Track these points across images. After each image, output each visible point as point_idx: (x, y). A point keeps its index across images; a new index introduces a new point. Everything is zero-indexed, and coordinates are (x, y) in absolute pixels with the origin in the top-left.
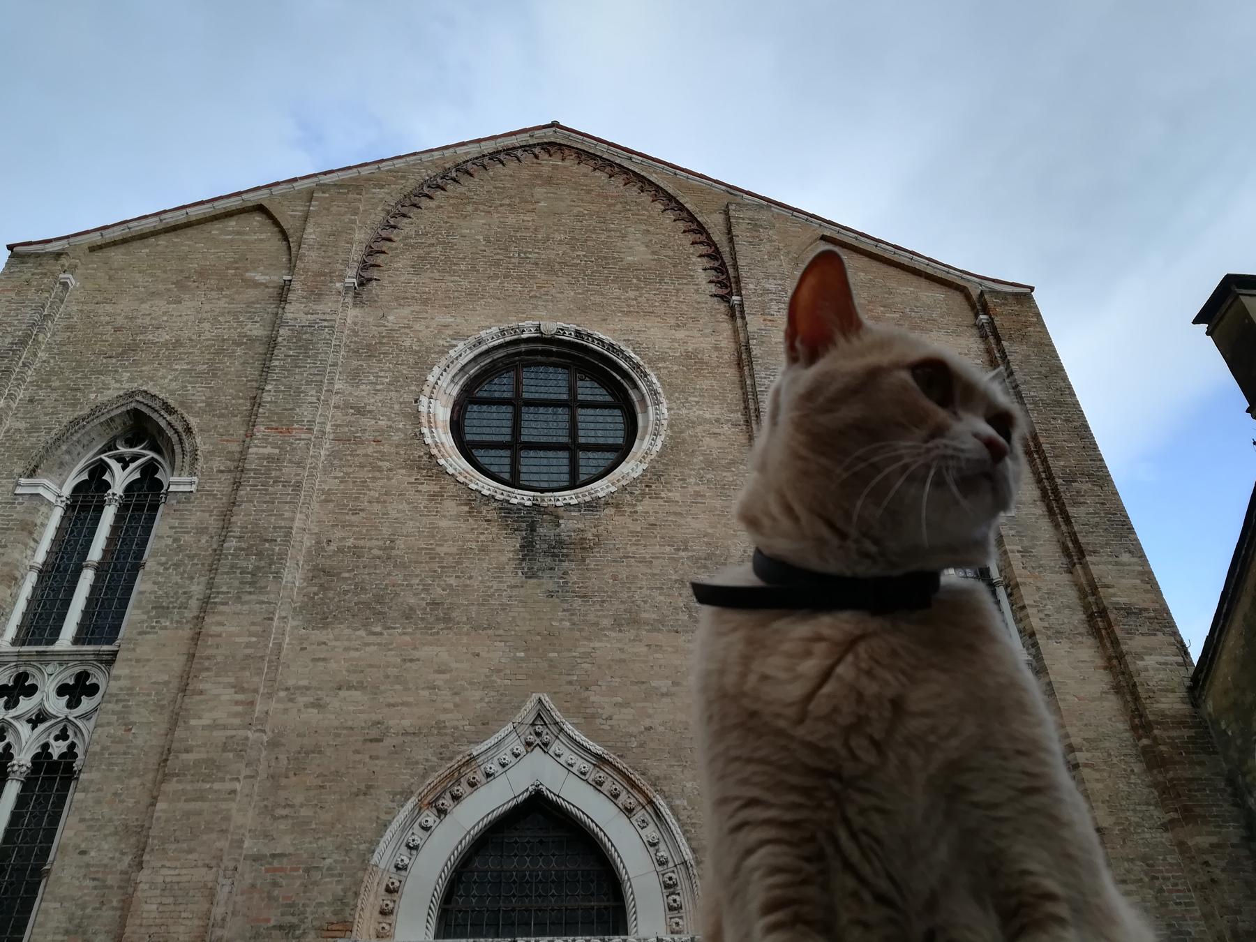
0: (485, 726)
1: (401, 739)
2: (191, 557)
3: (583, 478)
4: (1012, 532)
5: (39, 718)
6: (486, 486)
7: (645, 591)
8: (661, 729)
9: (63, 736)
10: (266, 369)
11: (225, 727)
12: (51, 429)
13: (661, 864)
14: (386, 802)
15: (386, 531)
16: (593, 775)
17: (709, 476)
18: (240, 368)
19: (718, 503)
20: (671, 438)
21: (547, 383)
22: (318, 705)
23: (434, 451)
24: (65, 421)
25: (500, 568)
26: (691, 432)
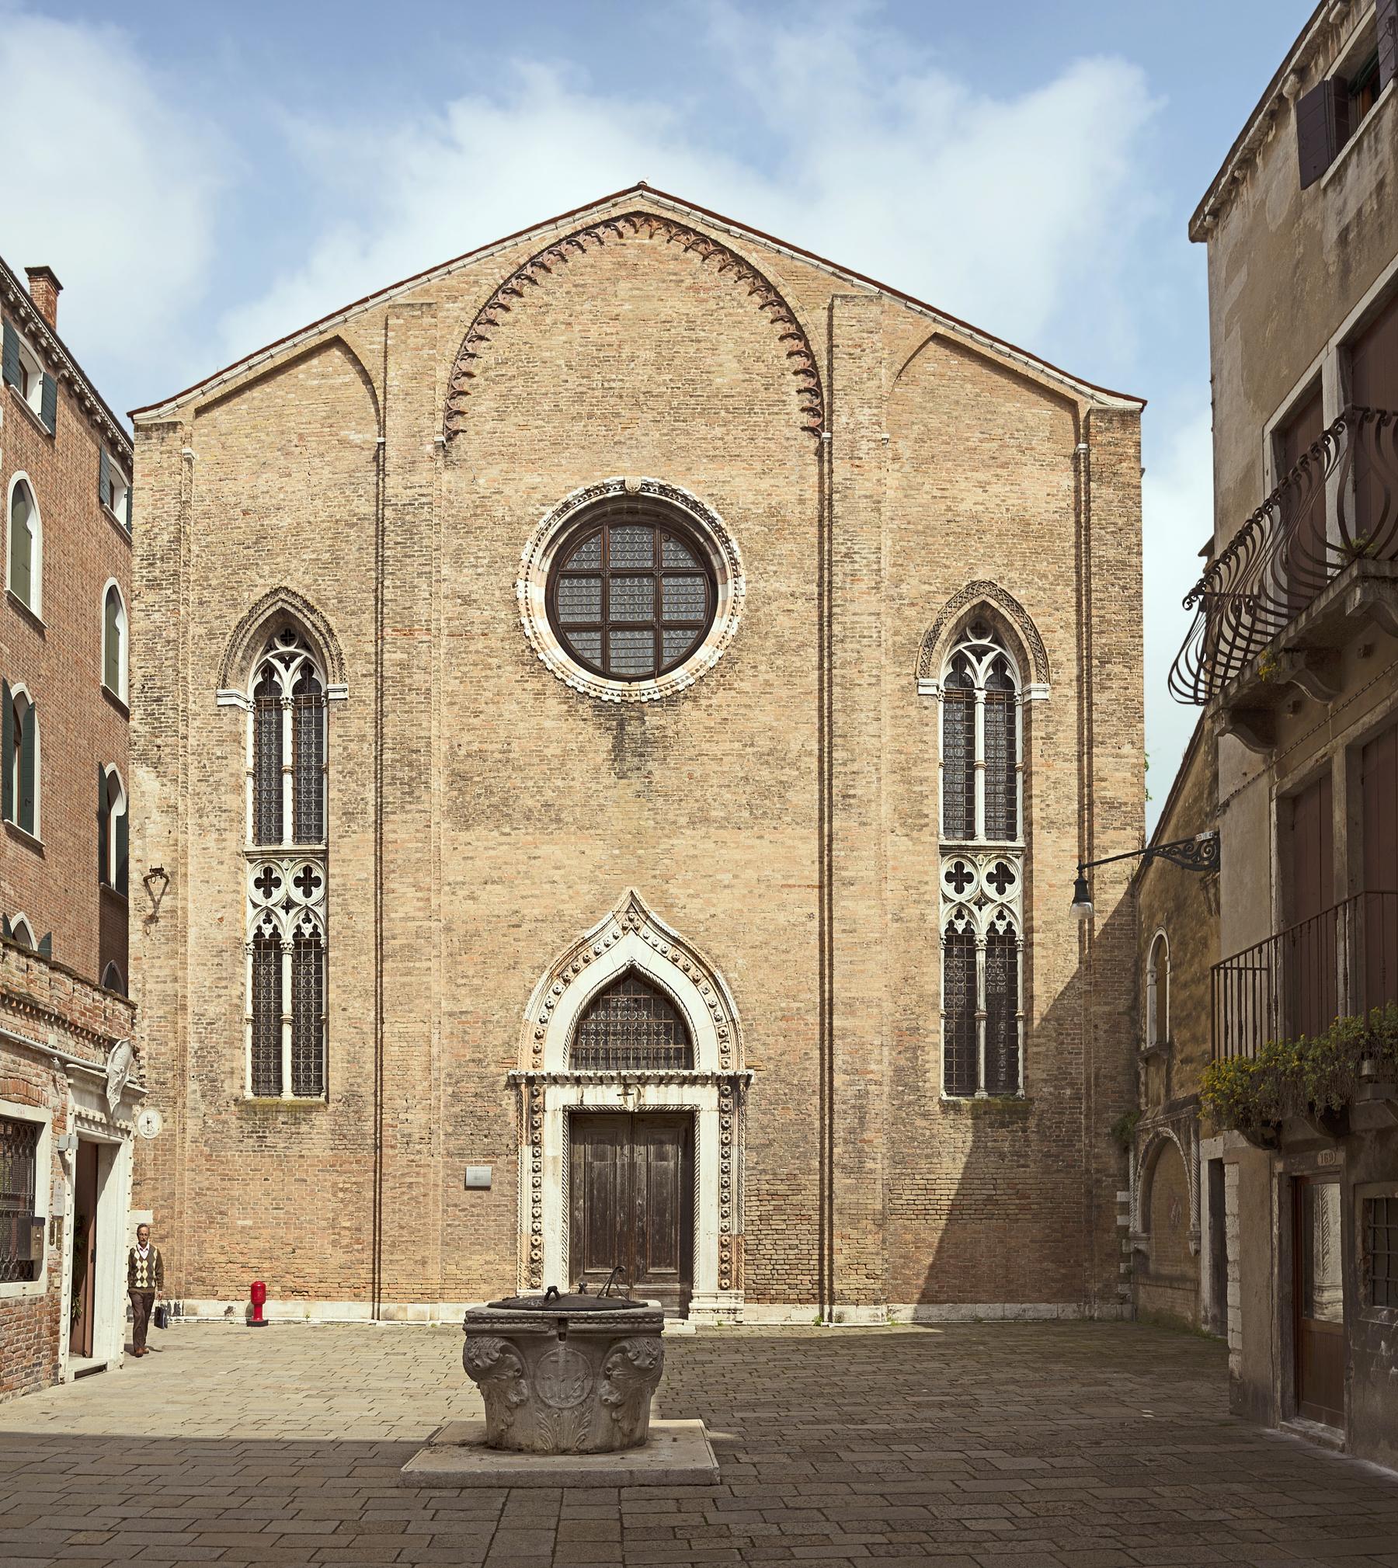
0: (592, 913)
1: (534, 924)
2: (360, 765)
3: (667, 662)
4: (1042, 717)
5: (289, 905)
6: (581, 678)
7: (716, 790)
8: (722, 916)
9: (307, 920)
10: (381, 560)
11: (414, 919)
12: (225, 634)
13: (717, 1020)
14: (529, 975)
15: (503, 734)
16: (672, 952)
17: (779, 662)
18: (357, 555)
19: (784, 693)
20: (747, 617)
21: (631, 547)
22: (472, 897)
23: (534, 645)
24: (234, 624)
25: (597, 770)
26: (766, 609)
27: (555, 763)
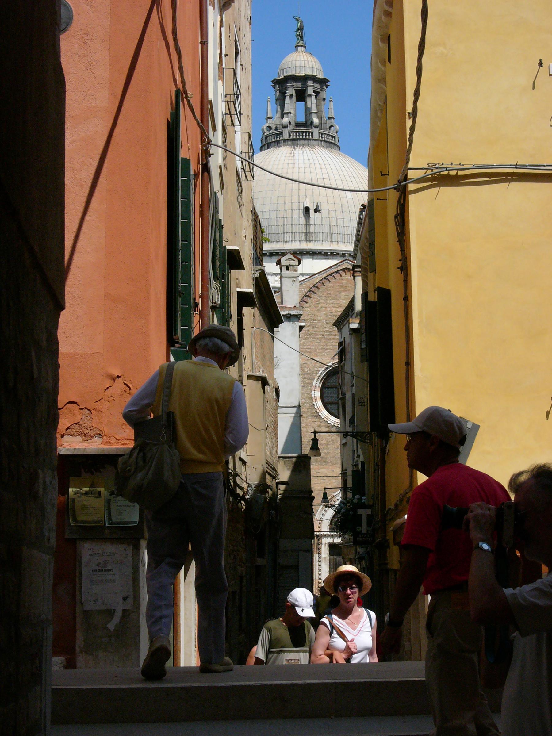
23: (318, 411)
27: (325, 445)
